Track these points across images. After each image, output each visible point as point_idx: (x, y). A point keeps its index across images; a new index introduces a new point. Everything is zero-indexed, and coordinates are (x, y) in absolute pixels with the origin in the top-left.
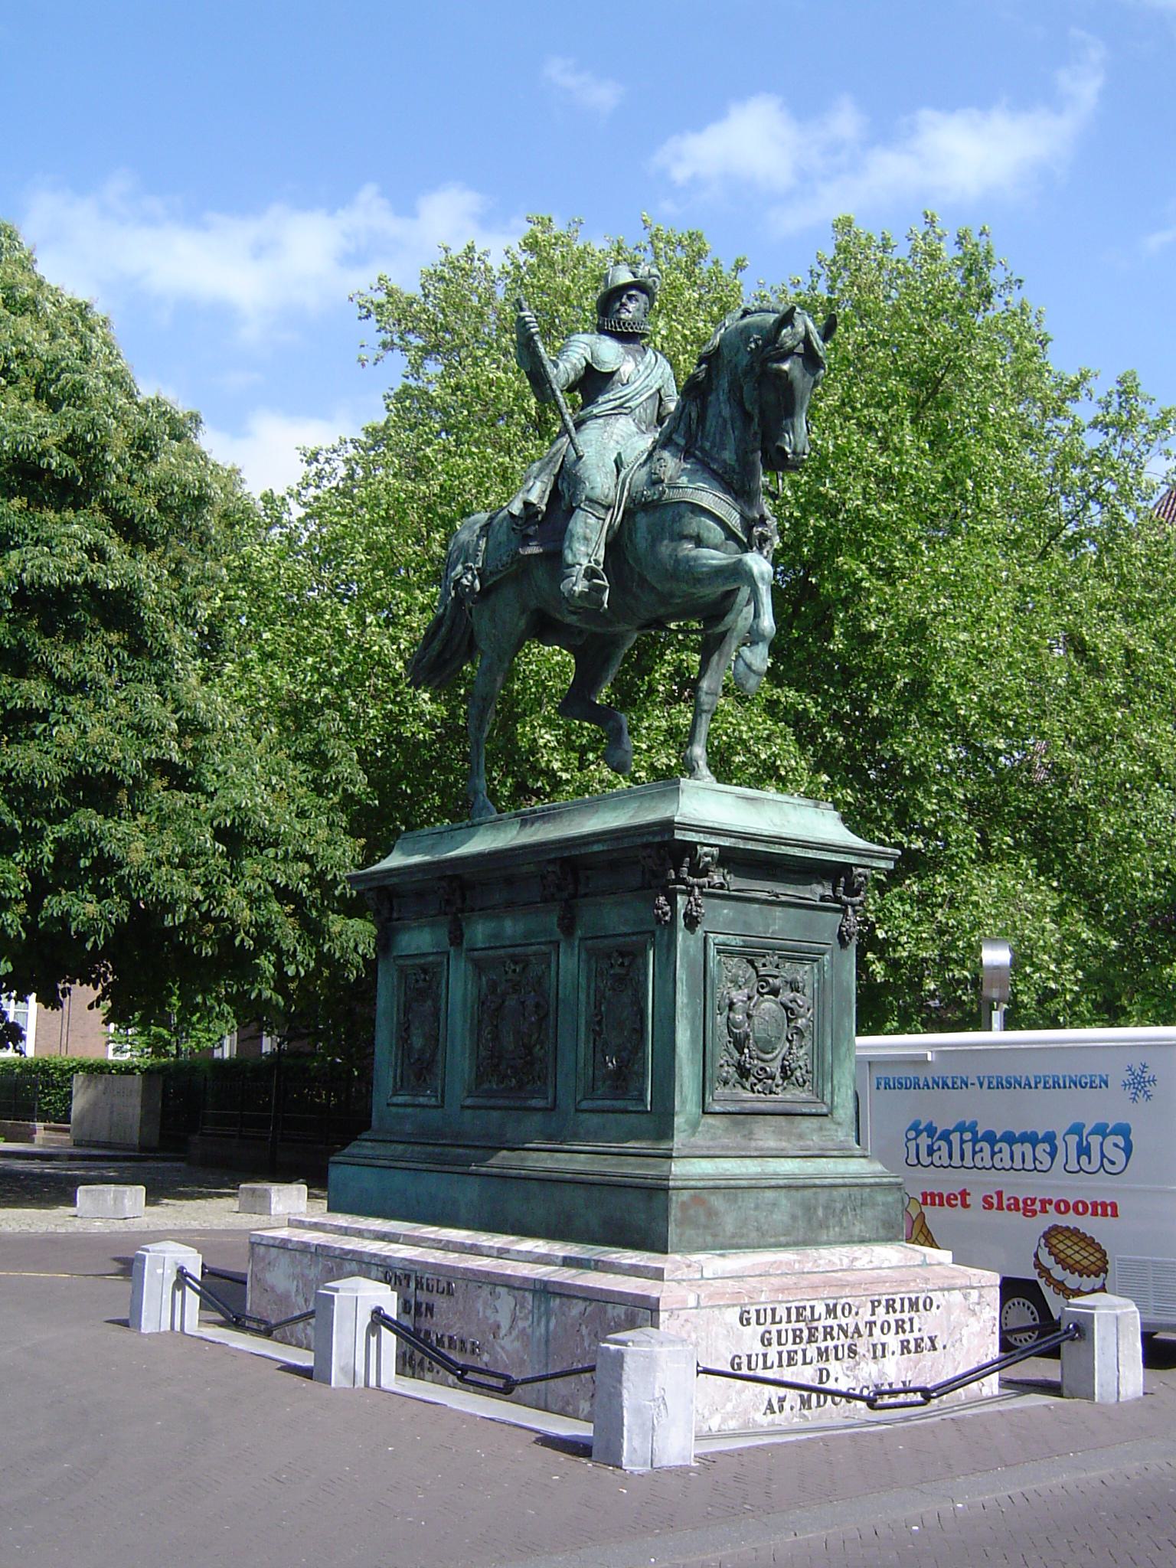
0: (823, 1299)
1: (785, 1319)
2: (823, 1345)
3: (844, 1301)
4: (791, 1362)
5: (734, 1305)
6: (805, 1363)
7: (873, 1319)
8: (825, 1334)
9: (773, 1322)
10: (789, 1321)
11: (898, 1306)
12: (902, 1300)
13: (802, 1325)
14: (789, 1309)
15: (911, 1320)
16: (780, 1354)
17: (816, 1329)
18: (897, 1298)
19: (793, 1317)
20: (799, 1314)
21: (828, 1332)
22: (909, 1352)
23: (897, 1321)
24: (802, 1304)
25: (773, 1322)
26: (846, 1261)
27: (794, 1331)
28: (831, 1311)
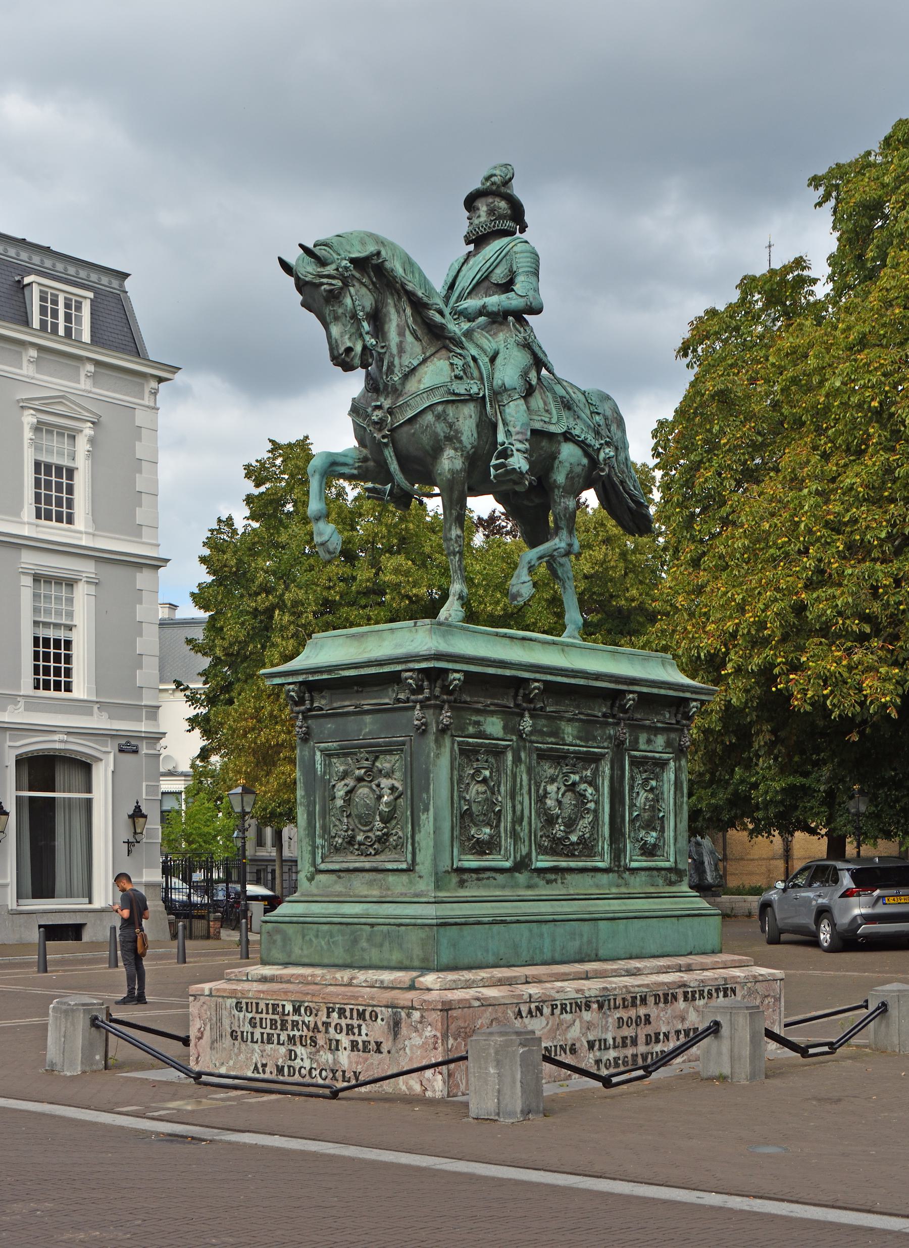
0: (292, 1001)
1: (264, 1011)
2: (292, 1033)
3: (306, 1004)
4: (270, 1041)
5: (231, 997)
6: (279, 1043)
7: (328, 1020)
8: (293, 1026)
9: (257, 1012)
10: (267, 1013)
11: (348, 1014)
12: (352, 1010)
13: (276, 1017)
14: (267, 1005)
15: (359, 1026)
16: (262, 1034)
17: (287, 1021)
18: (348, 1007)
19: (270, 1011)
20: (274, 1009)
21: (295, 1024)
22: (359, 1051)
23: (347, 1025)
24: (276, 1002)
25: (257, 1012)
26: (346, 979)
27: (271, 1020)
28: (297, 1010)
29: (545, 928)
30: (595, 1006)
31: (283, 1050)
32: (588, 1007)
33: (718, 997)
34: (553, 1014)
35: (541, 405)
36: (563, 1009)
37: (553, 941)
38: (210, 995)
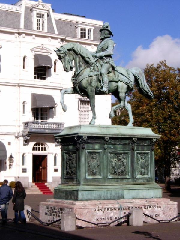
29: (108, 192)
30: (118, 209)
31: (52, 217)
32: (115, 209)
33: (155, 208)
34: (105, 211)
35: (113, 75)
36: (108, 209)
37: (111, 194)
38: (43, 205)
